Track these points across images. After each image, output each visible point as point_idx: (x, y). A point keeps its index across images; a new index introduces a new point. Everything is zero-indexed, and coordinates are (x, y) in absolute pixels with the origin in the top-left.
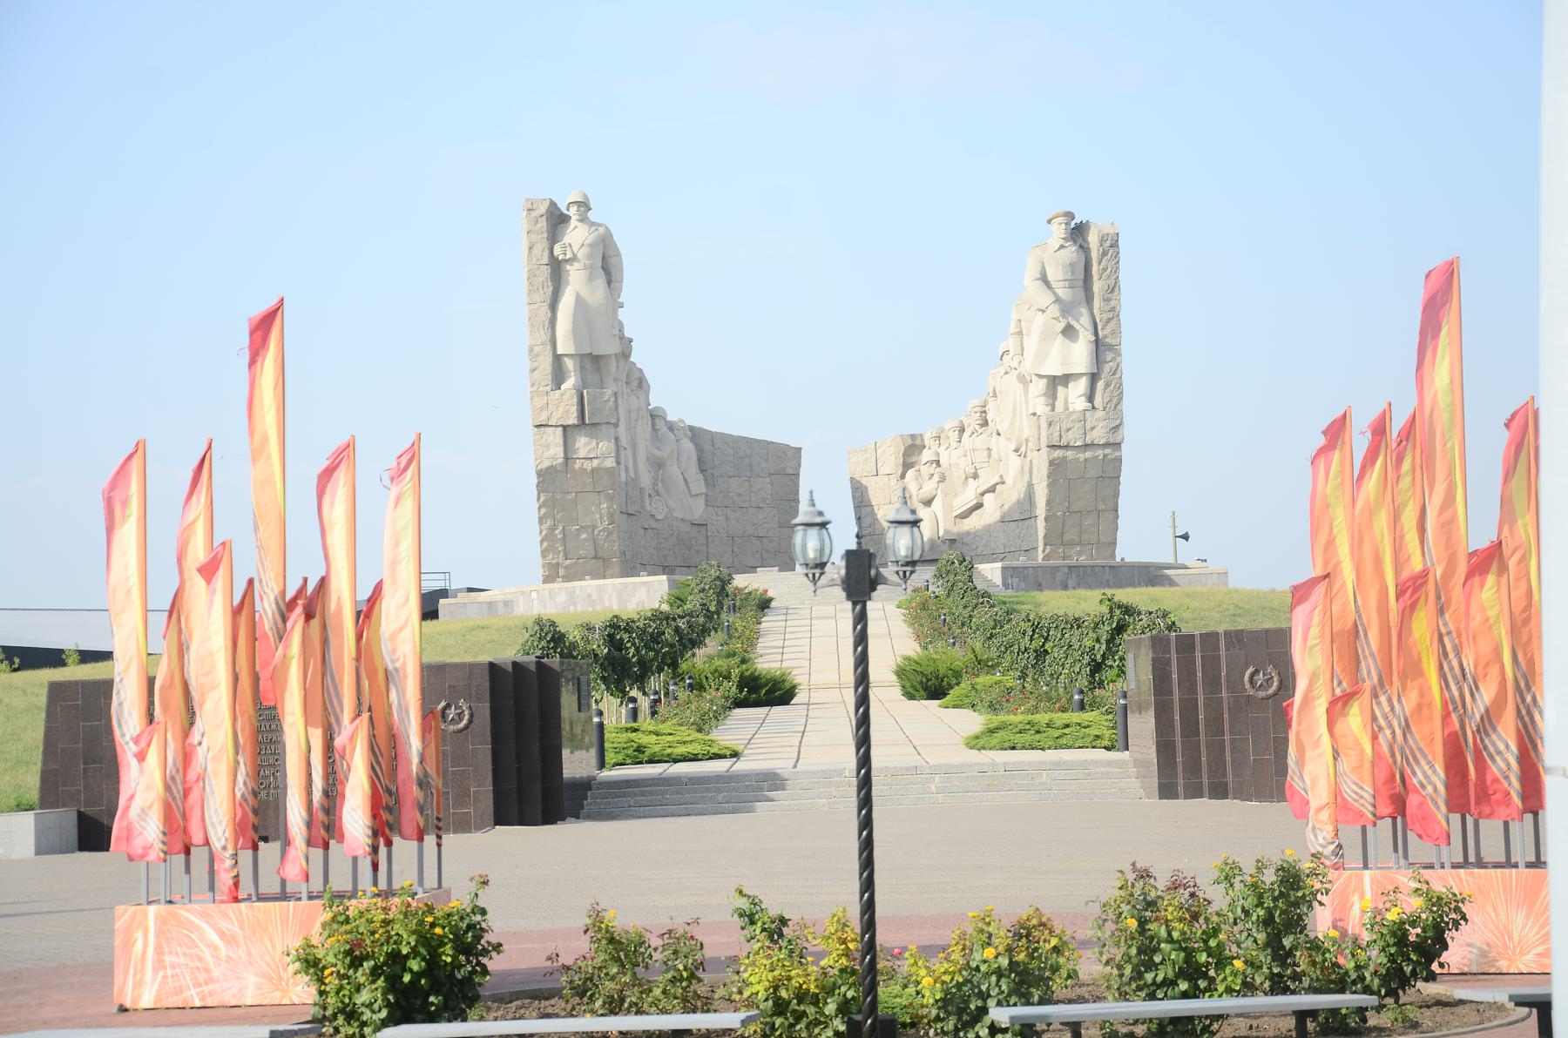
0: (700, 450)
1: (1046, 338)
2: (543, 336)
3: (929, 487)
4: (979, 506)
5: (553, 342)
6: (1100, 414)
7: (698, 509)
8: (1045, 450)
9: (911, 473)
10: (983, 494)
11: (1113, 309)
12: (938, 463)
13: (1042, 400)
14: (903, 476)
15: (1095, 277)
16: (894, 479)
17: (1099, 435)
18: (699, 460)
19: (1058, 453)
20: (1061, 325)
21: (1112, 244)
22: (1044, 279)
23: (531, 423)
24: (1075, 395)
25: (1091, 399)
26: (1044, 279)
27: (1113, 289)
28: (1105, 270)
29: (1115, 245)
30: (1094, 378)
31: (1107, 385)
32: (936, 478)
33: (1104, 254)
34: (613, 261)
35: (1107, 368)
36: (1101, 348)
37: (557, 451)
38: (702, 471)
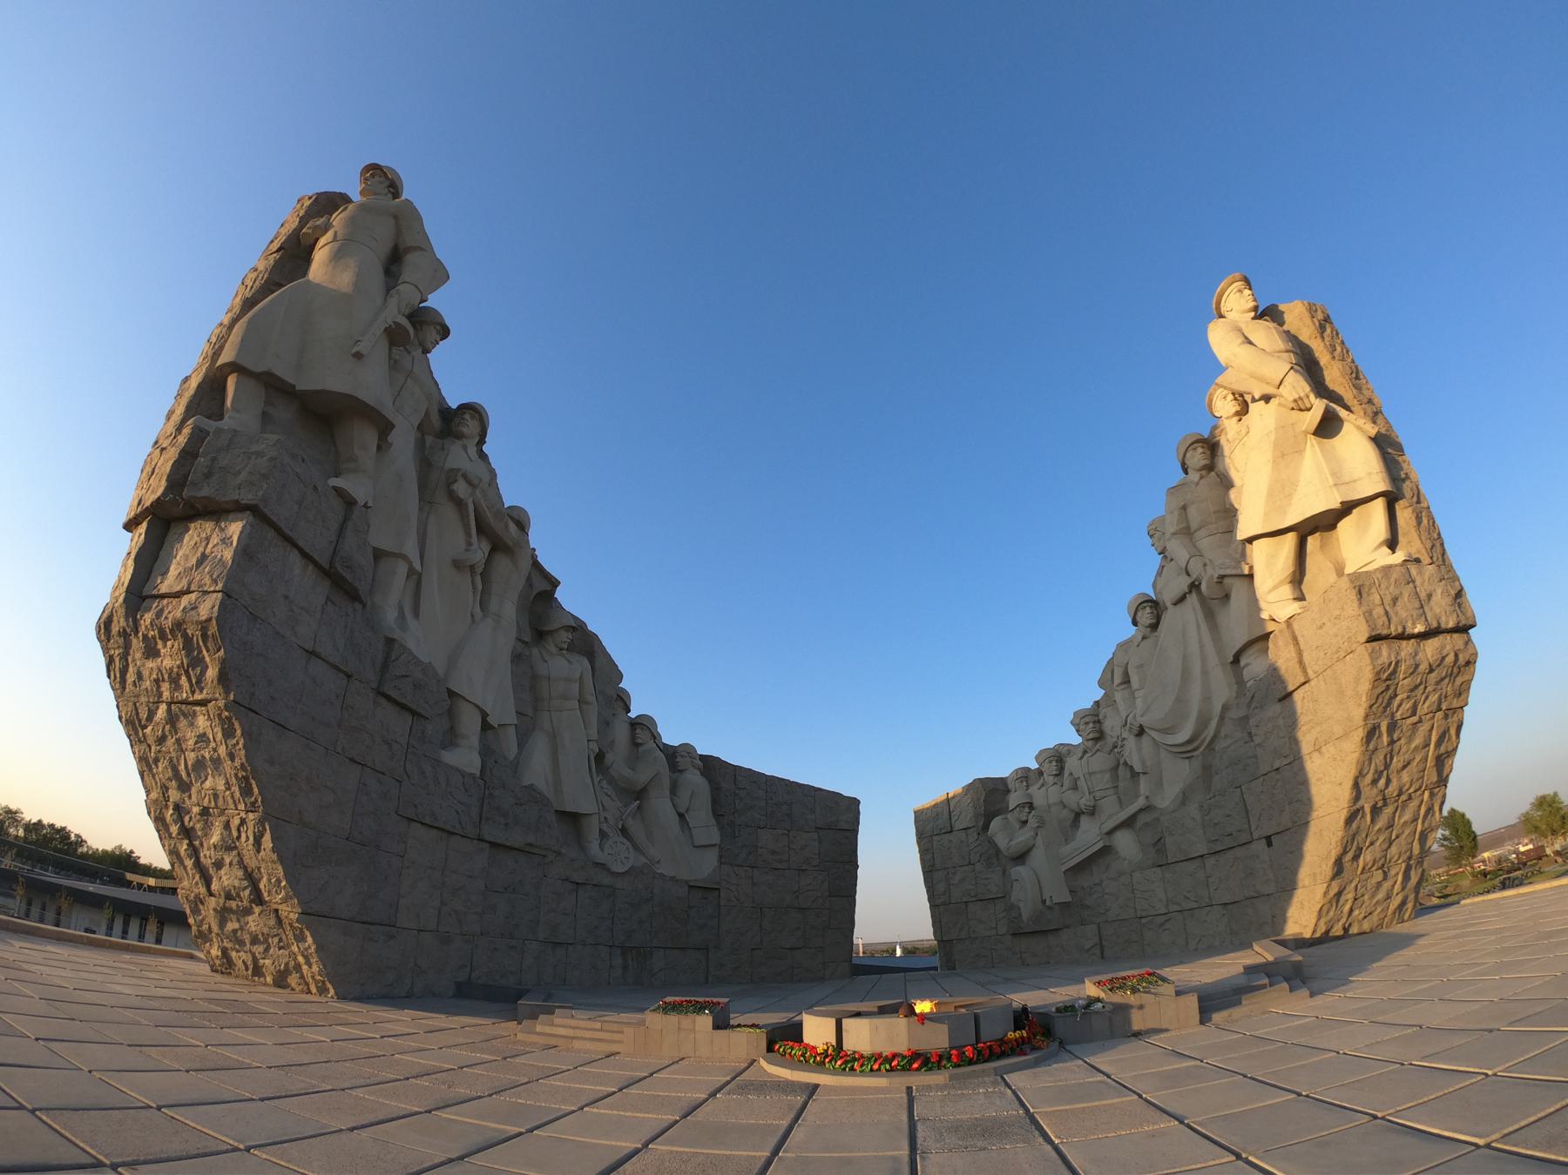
0: (715, 788)
1: (1285, 453)
3: (1023, 837)
4: (1106, 851)
7: (705, 866)
8: (1363, 652)
9: (996, 823)
10: (1110, 833)
12: (1031, 806)
13: (1287, 591)
14: (986, 827)
16: (973, 836)
17: (1441, 610)
18: (715, 802)
19: (1385, 652)
32: (1032, 823)
38: (717, 815)
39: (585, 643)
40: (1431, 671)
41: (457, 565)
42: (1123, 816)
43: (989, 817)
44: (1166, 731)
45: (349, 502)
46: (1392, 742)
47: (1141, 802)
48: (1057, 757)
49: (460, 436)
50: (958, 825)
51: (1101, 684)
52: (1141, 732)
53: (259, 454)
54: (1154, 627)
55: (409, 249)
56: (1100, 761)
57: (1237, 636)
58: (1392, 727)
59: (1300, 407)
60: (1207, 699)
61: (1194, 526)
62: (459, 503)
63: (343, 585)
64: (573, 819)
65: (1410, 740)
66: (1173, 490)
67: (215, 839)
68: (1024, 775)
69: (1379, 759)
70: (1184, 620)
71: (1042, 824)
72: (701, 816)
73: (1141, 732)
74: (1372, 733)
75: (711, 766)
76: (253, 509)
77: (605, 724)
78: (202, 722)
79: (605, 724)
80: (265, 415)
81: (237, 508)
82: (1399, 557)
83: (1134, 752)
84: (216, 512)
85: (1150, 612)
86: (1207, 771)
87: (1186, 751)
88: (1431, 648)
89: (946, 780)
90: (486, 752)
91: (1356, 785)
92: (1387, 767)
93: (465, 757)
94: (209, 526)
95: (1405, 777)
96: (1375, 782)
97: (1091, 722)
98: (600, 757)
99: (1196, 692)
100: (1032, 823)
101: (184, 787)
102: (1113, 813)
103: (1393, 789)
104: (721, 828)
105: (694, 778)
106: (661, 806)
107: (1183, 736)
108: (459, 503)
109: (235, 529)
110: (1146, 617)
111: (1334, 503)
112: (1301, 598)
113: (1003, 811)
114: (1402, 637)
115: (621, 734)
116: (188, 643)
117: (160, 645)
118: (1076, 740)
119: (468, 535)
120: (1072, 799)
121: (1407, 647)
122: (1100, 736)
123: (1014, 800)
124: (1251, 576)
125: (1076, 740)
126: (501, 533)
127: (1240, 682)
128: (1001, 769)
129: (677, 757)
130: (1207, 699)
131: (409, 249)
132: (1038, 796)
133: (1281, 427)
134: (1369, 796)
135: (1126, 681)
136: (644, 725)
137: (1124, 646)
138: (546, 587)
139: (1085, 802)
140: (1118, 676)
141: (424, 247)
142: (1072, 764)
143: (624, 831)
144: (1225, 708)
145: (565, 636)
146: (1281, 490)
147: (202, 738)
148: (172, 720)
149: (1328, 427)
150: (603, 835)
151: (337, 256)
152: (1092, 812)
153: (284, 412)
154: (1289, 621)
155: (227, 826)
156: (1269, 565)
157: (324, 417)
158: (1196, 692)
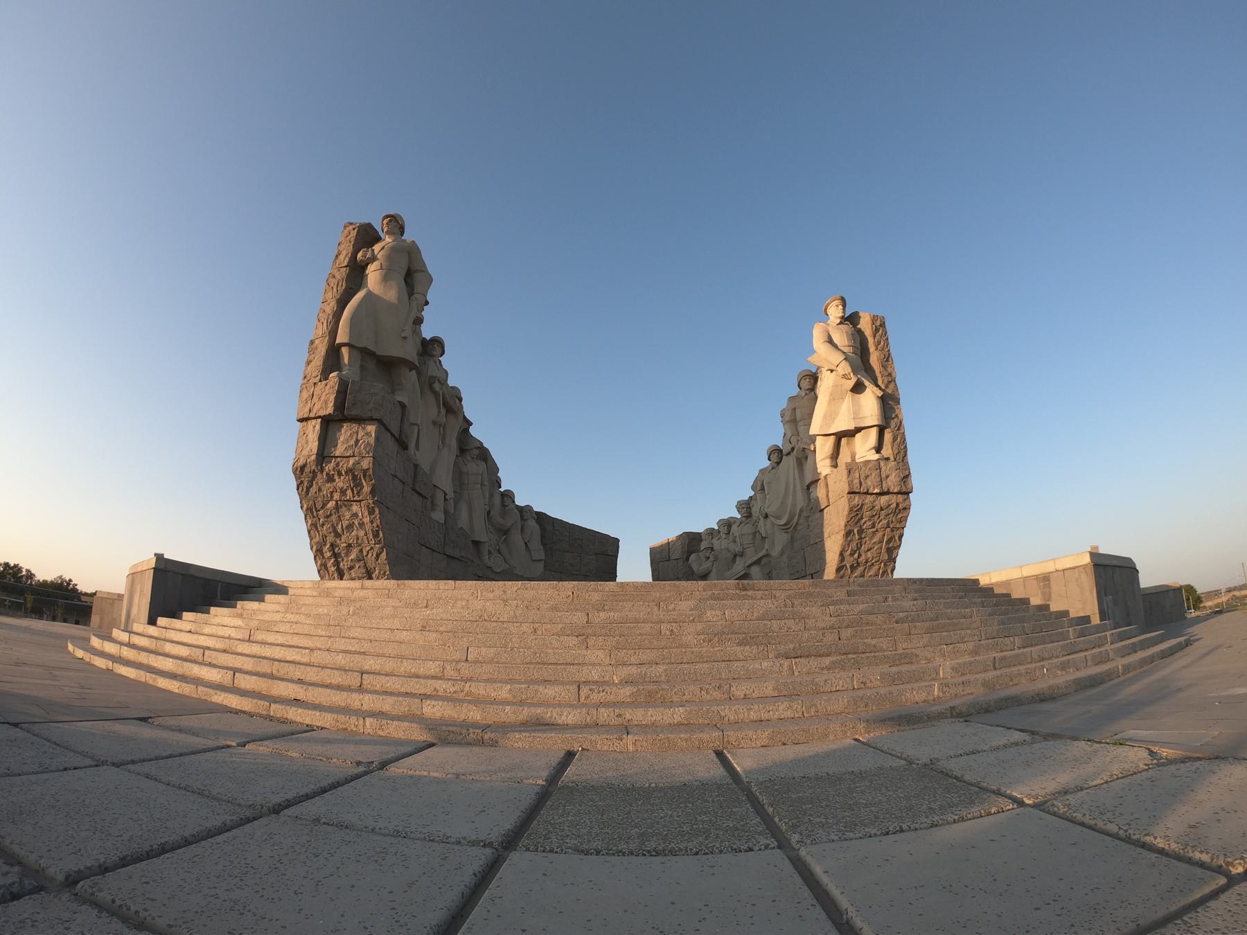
0: (543, 530)
1: (835, 399)
2: (323, 329)
3: (706, 565)
5: (333, 333)
6: (892, 464)
9: (693, 557)
10: (749, 566)
11: (890, 375)
12: (712, 549)
13: (828, 462)
14: (687, 559)
15: (872, 348)
17: (893, 483)
18: (543, 537)
20: (851, 384)
21: (880, 326)
22: (830, 341)
23: (295, 417)
24: (863, 448)
25: (878, 449)
26: (830, 341)
27: (887, 359)
28: (879, 343)
29: (883, 325)
30: (881, 430)
31: (895, 439)
32: (712, 558)
33: (877, 330)
34: (418, 276)
35: (893, 424)
36: (888, 403)
37: (314, 446)
38: (544, 545)
39: (484, 455)
40: (882, 509)
41: (434, 423)
42: (755, 558)
43: (690, 553)
44: (778, 518)
45: (403, 406)
46: (861, 538)
47: (764, 552)
48: (728, 524)
49: (432, 356)
50: (673, 557)
51: (753, 488)
52: (766, 516)
53: (376, 394)
54: (778, 463)
55: (416, 271)
56: (747, 529)
57: (808, 480)
58: (861, 532)
59: (845, 376)
60: (794, 505)
61: (798, 418)
62: (435, 393)
63: (403, 445)
64: (477, 544)
65: (871, 539)
66: (791, 399)
67: (353, 556)
68: (711, 532)
69: (853, 545)
70: (789, 462)
71: (716, 559)
72: (536, 544)
73: (766, 516)
74: (848, 534)
75: (541, 517)
76: (380, 422)
77: (491, 495)
78: (355, 508)
79: (491, 495)
80: (362, 367)
81: (371, 420)
82: (877, 456)
83: (763, 526)
84: (359, 420)
85: (777, 454)
86: (792, 540)
87: (786, 527)
88: (883, 500)
89: (668, 532)
90: (446, 512)
91: (841, 554)
92: (858, 549)
93: (438, 516)
94: (355, 426)
95: (869, 554)
96: (852, 555)
97: (746, 507)
98: (489, 513)
99: (790, 501)
100: (712, 558)
101: (338, 535)
102: (752, 557)
103: (862, 559)
104: (546, 551)
105: (532, 524)
106: (517, 538)
107: (783, 522)
108: (435, 393)
109: (371, 428)
110: (775, 457)
111: (851, 427)
112: (835, 466)
113: (697, 551)
114: (867, 493)
115: (497, 500)
116: (355, 478)
117: (336, 477)
118: (739, 516)
119: (439, 408)
120: (732, 547)
121: (869, 499)
122: (749, 516)
123: (703, 545)
124: (815, 451)
125: (739, 516)
126: (451, 403)
127: (809, 499)
128: (699, 528)
129: (525, 511)
130: (794, 505)
131: (416, 271)
132: (717, 544)
133: (835, 386)
134: (849, 561)
135: (763, 489)
136: (508, 495)
137: (762, 471)
138: (465, 426)
139: (738, 549)
140: (760, 486)
141: (424, 270)
142: (734, 528)
143: (499, 551)
144: (801, 511)
145: (476, 452)
146: (831, 416)
147: (355, 515)
148: (337, 508)
149: (858, 388)
150: (490, 552)
151: (386, 278)
152: (742, 555)
153: (371, 365)
154: (826, 477)
155: (361, 551)
156: (823, 448)
157: (388, 366)
158: (790, 501)
